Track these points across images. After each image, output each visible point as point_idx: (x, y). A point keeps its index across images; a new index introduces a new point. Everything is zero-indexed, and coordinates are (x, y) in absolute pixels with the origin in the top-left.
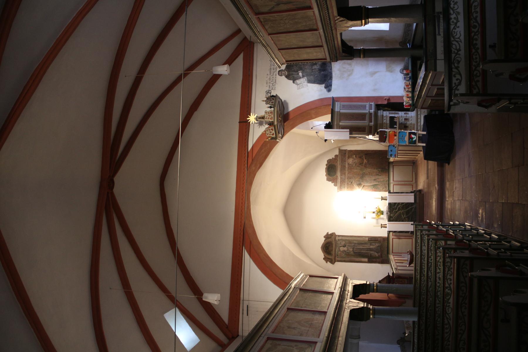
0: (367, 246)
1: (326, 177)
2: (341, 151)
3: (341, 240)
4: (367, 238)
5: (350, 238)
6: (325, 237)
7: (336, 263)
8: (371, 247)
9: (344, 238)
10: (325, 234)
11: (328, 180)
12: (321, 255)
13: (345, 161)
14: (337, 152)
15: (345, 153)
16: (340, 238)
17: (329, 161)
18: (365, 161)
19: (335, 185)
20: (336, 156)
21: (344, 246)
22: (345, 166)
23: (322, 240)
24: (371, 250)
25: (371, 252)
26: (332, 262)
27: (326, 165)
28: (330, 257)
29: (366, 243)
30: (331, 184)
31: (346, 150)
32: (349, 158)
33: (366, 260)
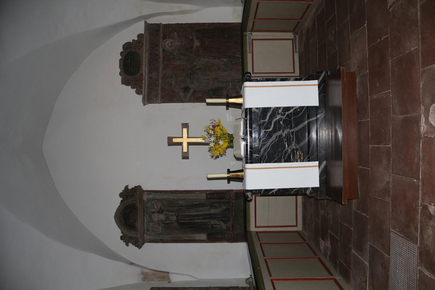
0: (205, 211)
1: (119, 78)
2: (148, 27)
3: (154, 199)
4: (204, 196)
5: (171, 197)
6: (121, 195)
7: (146, 245)
8: (213, 211)
9: (159, 196)
10: (122, 189)
11: (125, 82)
12: (117, 232)
13: (158, 45)
14: (140, 28)
15: (158, 30)
16: (151, 196)
17: (127, 46)
18: (197, 43)
19: (138, 93)
20: (140, 36)
21: (161, 211)
22: (157, 55)
23: (117, 202)
24: (212, 217)
25: (213, 222)
26: (139, 245)
27: (121, 54)
28: (132, 234)
29: (201, 205)
30: (130, 91)
31: (158, 25)
32: (164, 38)
33: (204, 236)
